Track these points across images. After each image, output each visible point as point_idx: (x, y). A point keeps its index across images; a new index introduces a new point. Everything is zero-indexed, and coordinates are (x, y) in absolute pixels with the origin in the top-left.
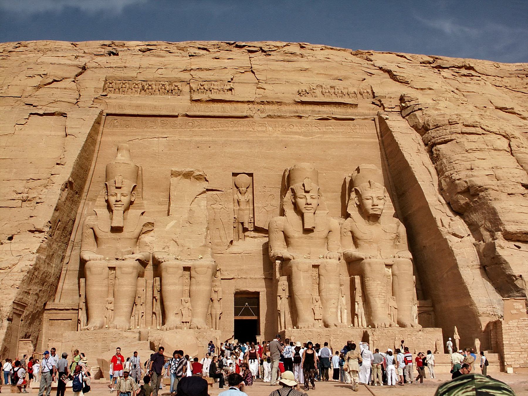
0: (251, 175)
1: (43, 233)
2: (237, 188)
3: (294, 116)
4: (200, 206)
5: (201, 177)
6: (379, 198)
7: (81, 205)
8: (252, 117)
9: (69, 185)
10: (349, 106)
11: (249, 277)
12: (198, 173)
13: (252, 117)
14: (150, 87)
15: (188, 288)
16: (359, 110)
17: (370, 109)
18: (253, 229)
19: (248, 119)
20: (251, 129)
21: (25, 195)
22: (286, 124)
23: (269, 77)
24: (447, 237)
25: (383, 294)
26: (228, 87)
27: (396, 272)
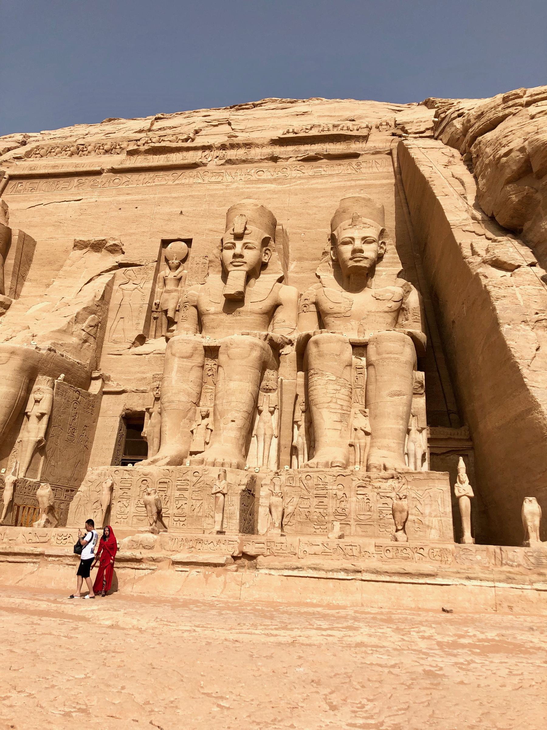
0: (189, 242)
2: (167, 260)
5: (117, 248)
6: (365, 240)
8: (205, 165)
12: (111, 243)
13: (205, 165)
14: (85, 149)
16: (370, 144)
17: (387, 141)
20: (200, 181)
22: (253, 171)
24: (479, 270)
25: (339, 402)
26: (186, 137)
27: (373, 358)
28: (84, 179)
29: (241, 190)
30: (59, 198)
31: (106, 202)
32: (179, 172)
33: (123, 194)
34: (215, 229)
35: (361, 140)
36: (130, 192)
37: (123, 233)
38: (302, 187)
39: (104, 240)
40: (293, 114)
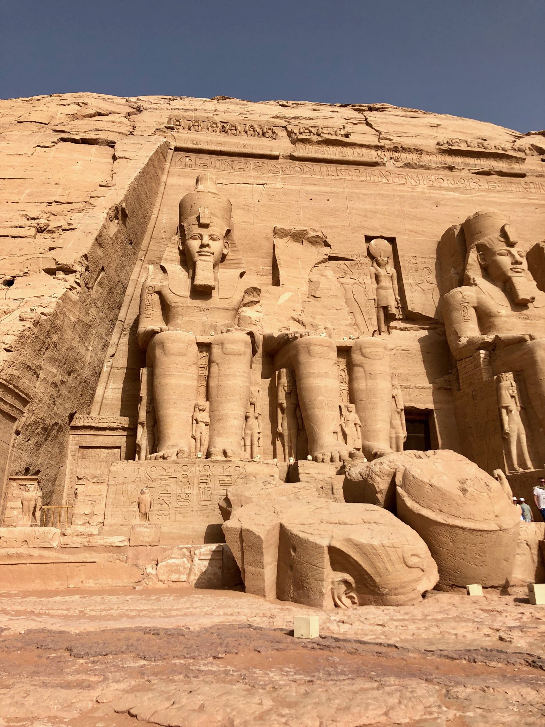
0: (392, 241)
1: (74, 274)
3: (443, 167)
4: (325, 276)
7: (136, 269)
8: (384, 165)
9: (120, 214)
10: (514, 160)
11: (412, 385)
13: (384, 165)
14: (234, 128)
15: (346, 387)
18: (401, 317)
19: (379, 167)
20: (385, 180)
21: (42, 222)
22: (433, 177)
23: (391, 130)
28: (260, 161)
29: (427, 195)
30: (238, 179)
31: (295, 190)
32: (362, 168)
33: (310, 184)
34: (414, 230)
35: (520, 162)
36: (316, 183)
37: (322, 225)
38: (483, 199)
39: (306, 230)
40: (428, 124)
